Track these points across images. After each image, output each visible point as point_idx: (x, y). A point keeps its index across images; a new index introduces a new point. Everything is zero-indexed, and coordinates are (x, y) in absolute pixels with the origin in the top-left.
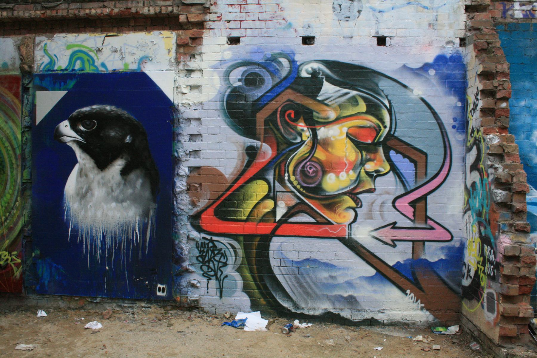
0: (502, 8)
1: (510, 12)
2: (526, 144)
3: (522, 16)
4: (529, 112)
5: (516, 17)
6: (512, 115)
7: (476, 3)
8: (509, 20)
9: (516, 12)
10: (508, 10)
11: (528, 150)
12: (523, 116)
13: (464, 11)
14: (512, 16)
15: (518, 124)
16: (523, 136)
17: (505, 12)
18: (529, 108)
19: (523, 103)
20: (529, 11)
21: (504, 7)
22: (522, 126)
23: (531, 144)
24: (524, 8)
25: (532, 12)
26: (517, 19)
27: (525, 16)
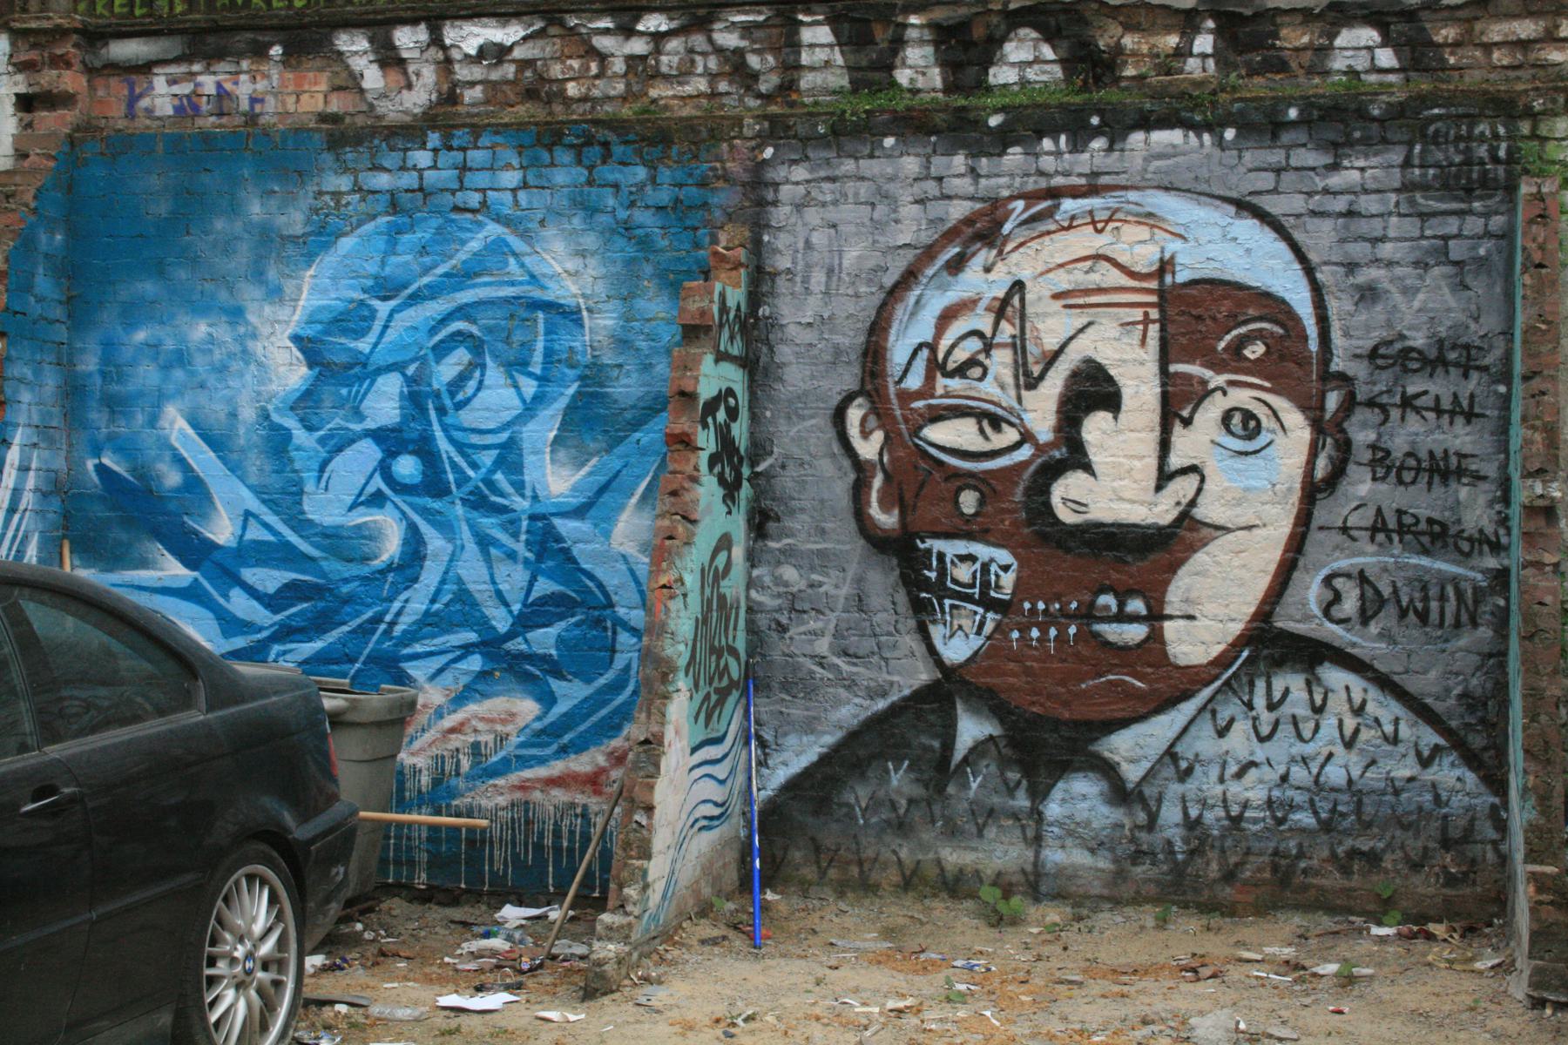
0: (126, 92)
1: (144, 103)
2: (148, 438)
3: (170, 112)
4: (155, 359)
5: (158, 113)
6: (117, 366)
7: (36, 89)
8: (142, 122)
9: (158, 101)
10: (141, 96)
11: (153, 453)
12: (141, 369)
13: (10, 109)
14: (149, 112)
15: (131, 388)
16: (140, 418)
17: (133, 100)
18: (154, 347)
19: (141, 336)
20: (187, 96)
21: (132, 90)
22: (141, 394)
23: (159, 438)
24: (176, 89)
25: (195, 99)
26: (159, 118)
27: (179, 110)
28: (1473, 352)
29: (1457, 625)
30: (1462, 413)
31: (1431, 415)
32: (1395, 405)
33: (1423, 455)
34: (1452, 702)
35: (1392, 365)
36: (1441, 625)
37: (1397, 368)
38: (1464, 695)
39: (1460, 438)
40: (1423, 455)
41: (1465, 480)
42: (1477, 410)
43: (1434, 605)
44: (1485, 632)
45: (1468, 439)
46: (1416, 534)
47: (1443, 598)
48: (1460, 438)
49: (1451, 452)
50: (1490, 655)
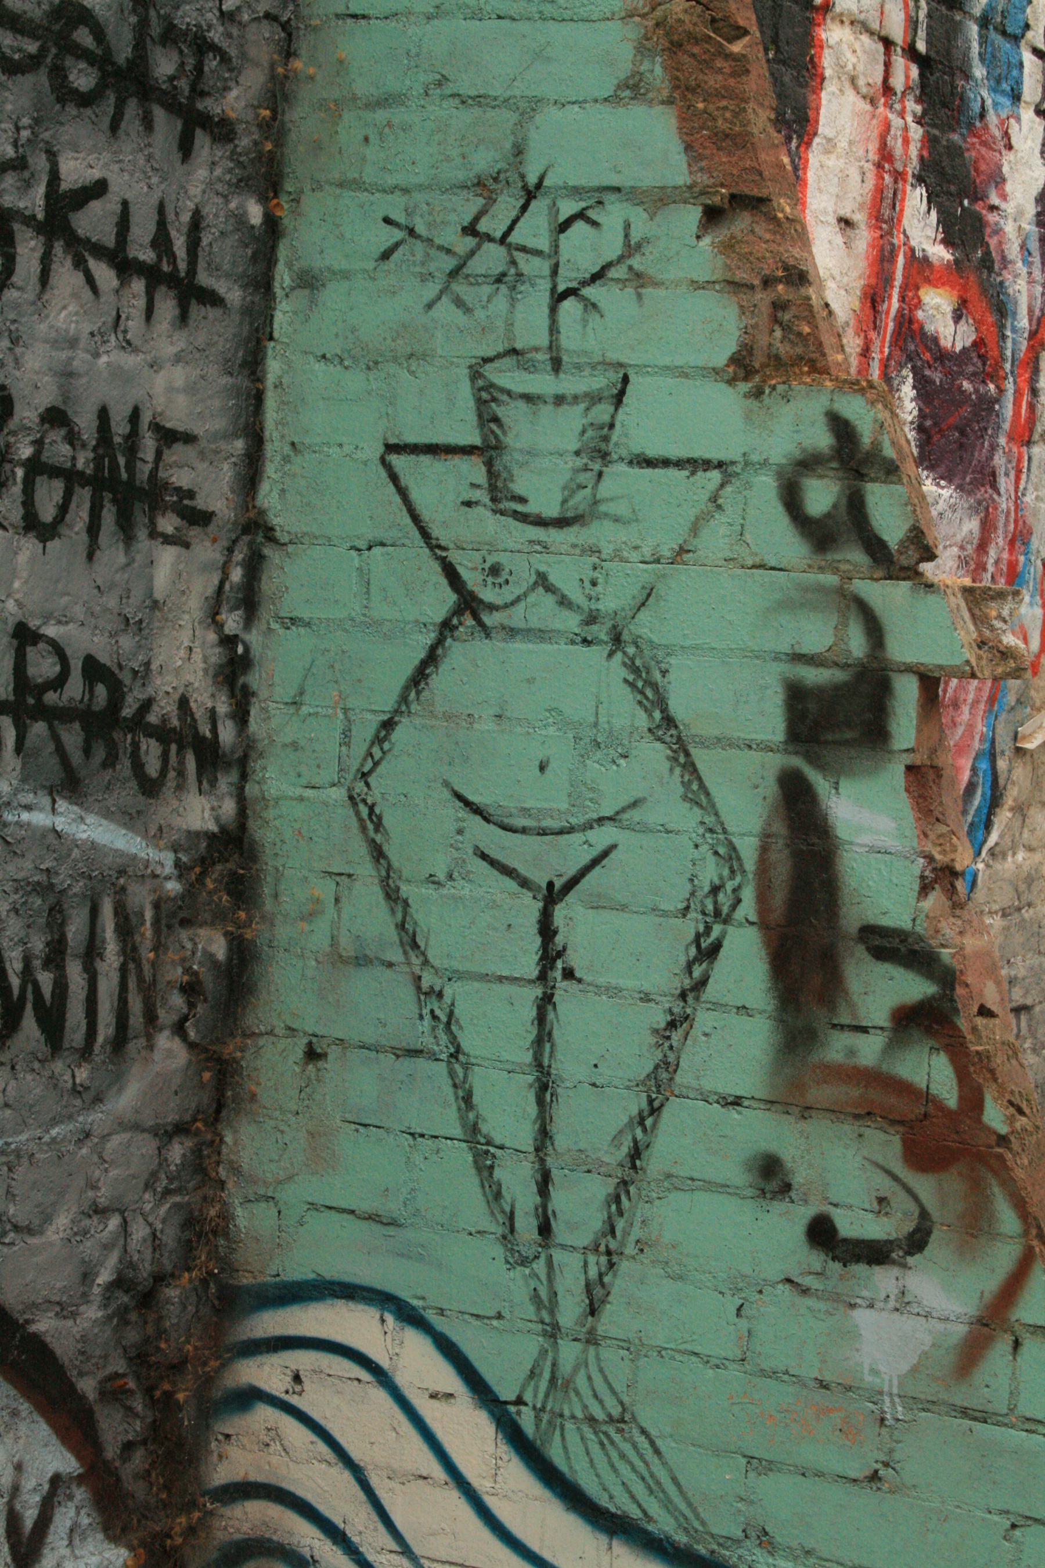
28: (212, 63)
29: (119, 1042)
30: (172, 280)
31: (104, 274)
32: (29, 220)
33: (86, 422)
34: (92, 1312)
35: (32, 63)
36: (86, 1052)
37: (41, 78)
38: (119, 1283)
39: (168, 375)
40: (86, 422)
41: (168, 524)
42: (203, 279)
43: (75, 972)
44: (170, 1053)
45: (179, 375)
46: (54, 716)
47: (92, 952)
48: (168, 375)
49: (146, 418)
50: (180, 1129)
